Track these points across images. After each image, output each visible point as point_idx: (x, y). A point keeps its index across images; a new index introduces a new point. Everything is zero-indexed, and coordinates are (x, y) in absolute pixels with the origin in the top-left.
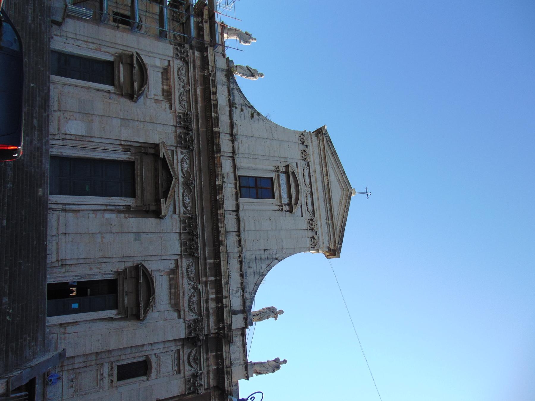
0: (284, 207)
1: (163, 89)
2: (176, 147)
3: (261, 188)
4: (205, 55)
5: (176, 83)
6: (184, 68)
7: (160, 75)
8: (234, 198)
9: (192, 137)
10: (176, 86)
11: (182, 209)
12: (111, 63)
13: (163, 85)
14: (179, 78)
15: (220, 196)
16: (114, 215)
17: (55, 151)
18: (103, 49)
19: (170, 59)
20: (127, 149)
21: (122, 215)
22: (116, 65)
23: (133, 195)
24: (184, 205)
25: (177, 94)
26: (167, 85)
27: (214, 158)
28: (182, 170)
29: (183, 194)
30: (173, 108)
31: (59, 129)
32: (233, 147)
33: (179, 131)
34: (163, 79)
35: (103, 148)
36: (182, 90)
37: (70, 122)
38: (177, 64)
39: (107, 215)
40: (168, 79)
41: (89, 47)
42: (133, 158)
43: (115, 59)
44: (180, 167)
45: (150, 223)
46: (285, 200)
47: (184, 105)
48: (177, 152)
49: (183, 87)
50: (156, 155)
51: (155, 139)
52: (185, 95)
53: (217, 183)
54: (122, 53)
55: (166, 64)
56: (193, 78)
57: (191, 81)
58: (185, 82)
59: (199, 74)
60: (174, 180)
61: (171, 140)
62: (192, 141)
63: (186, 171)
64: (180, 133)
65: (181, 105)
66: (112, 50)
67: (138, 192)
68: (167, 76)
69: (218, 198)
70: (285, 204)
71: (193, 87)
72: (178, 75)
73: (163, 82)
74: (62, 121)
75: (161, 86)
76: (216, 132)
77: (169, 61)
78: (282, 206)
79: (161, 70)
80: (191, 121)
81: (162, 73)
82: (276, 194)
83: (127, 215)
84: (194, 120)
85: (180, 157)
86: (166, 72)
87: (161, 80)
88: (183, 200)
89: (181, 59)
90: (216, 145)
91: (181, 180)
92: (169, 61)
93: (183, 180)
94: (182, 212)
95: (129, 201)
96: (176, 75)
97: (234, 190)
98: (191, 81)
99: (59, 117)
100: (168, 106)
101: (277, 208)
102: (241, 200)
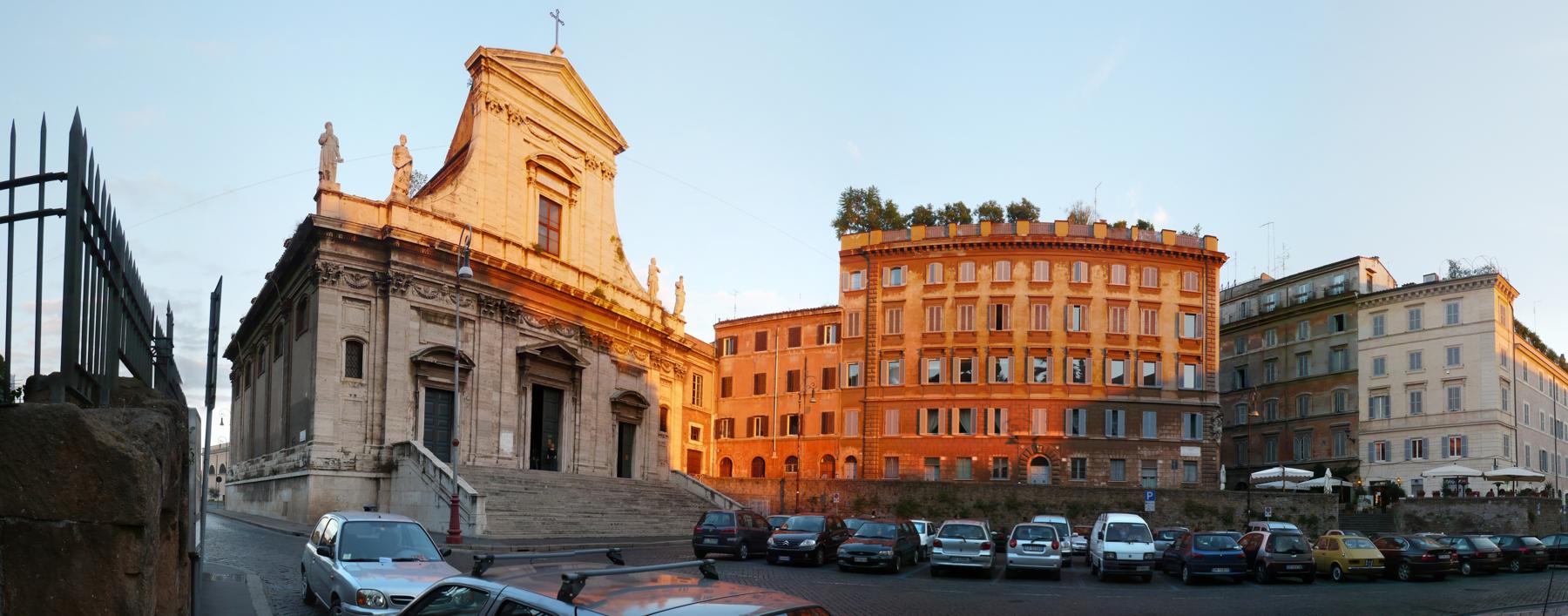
0: (573, 197)
1: (448, 326)
2: (518, 327)
3: (548, 219)
4: (398, 244)
5: (440, 304)
6: (420, 286)
7: (430, 326)
8: (565, 268)
9: (508, 303)
10: (445, 305)
11: (572, 340)
12: (428, 390)
13: (443, 325)
14: (433, 298)
15: (572, 291)
16: (578, 415)
17: (528, 465)
18: (412, 398)
19: (409, 304)
20: (522, 391)
21: (578, 407)
22: (431, 386)
23: (560, 393)
24: (570, 337)
25: (454, 307)
26: (444, 318)
27: (534, 282)
28: (539, 328)
29: (561, 335)
30: (473, 318)
31: (510, 459)
32: (514, 244)
33: (499, 319)
34: (435, 323)
35: (523, 417)
36: (448, 297)
37: (501, 447)
38: (411, 294)
39: (577, 423)
40: (436, 315)
41: (412, 416)
42: (531, 385)
43: (423, 385)
44: (536, 330)
45: (588, 380)
46: (563, 189)
47: (467, 300)
48: (522, 329)
49: (444, 295)
50: (533, 357)
51: (510, 354)
52: (454, 295)
53: (559, 289)
54: (411, 374)
55: (414, 313)
56: (432, 276)
57: (437, 280)
58: (436, 290)
59: (424, 264)
60: (560, 346)
61: (508, 330)
62: (513, 304)
63: (540, 322)
64: (502, 318)
65: (468, 305)
66: (411, 389)
67: (560, 386)
68: (431, 315)
69: (573, 294)
70: (571, 194)
71: (444, 279)
72: (429, 298)
73: (439, 324)
74: (501, 455)
75: (443, 328)
76: (507, 268)
77: (412, 307)
78: (573, 200)
79: (423, 323)
80: (490, 298)
81: (429, 322)
82: (557, 199)
83: (578, 403)
84: (486, 293)
85: (525, 325)
86: (427, 316)
87: (436, 326)
88: (565, 336)
89: (407, 286)
90: (522, 273)
91: (547, 332)
92: (412, 307)
93: (547, 331)
94: (575, 342)
95: (567, 398)
96: (429, 301)
97: (558, 265)
98: (437, 280)
99: (498, 458)
100: (470, 326)
101: (573, 209)
102: (563, 258)
